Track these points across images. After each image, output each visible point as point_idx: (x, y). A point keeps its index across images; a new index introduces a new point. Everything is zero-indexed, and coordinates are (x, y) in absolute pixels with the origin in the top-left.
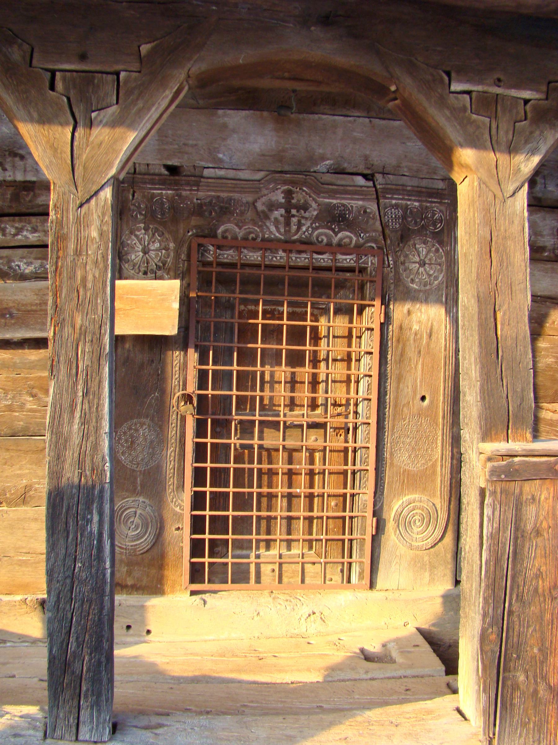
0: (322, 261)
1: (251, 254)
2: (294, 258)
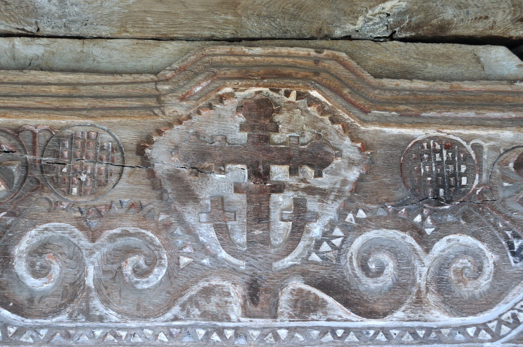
0: (381, 337)
1: (133, 324)
2: (283, 333)
